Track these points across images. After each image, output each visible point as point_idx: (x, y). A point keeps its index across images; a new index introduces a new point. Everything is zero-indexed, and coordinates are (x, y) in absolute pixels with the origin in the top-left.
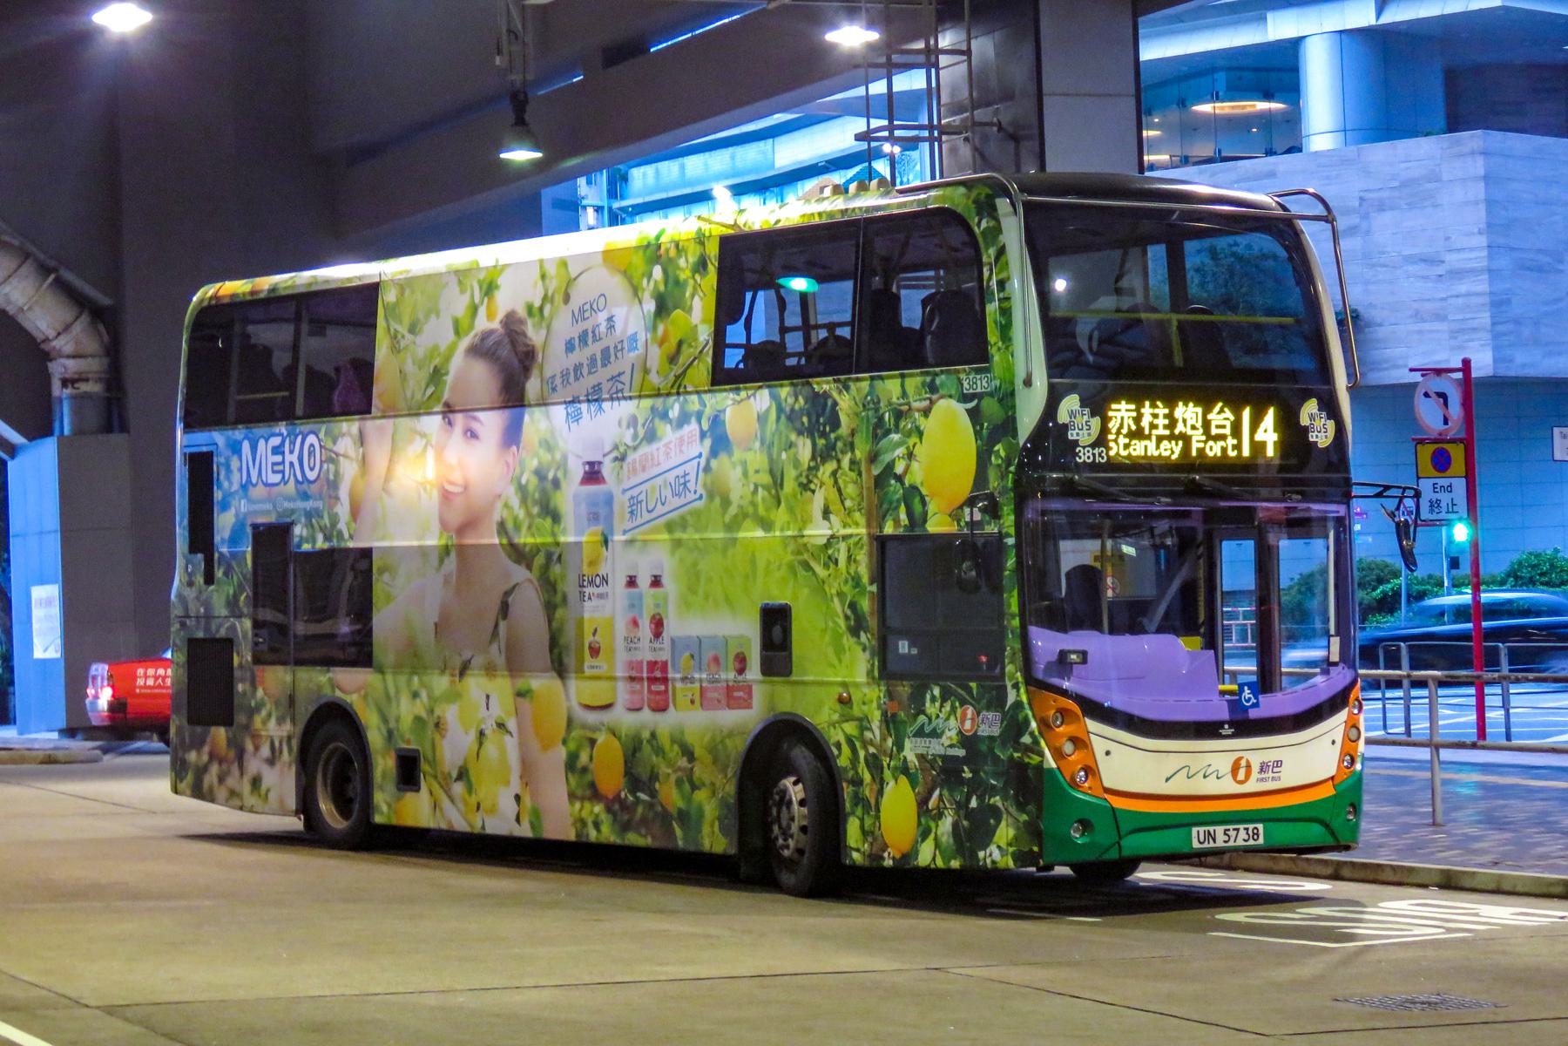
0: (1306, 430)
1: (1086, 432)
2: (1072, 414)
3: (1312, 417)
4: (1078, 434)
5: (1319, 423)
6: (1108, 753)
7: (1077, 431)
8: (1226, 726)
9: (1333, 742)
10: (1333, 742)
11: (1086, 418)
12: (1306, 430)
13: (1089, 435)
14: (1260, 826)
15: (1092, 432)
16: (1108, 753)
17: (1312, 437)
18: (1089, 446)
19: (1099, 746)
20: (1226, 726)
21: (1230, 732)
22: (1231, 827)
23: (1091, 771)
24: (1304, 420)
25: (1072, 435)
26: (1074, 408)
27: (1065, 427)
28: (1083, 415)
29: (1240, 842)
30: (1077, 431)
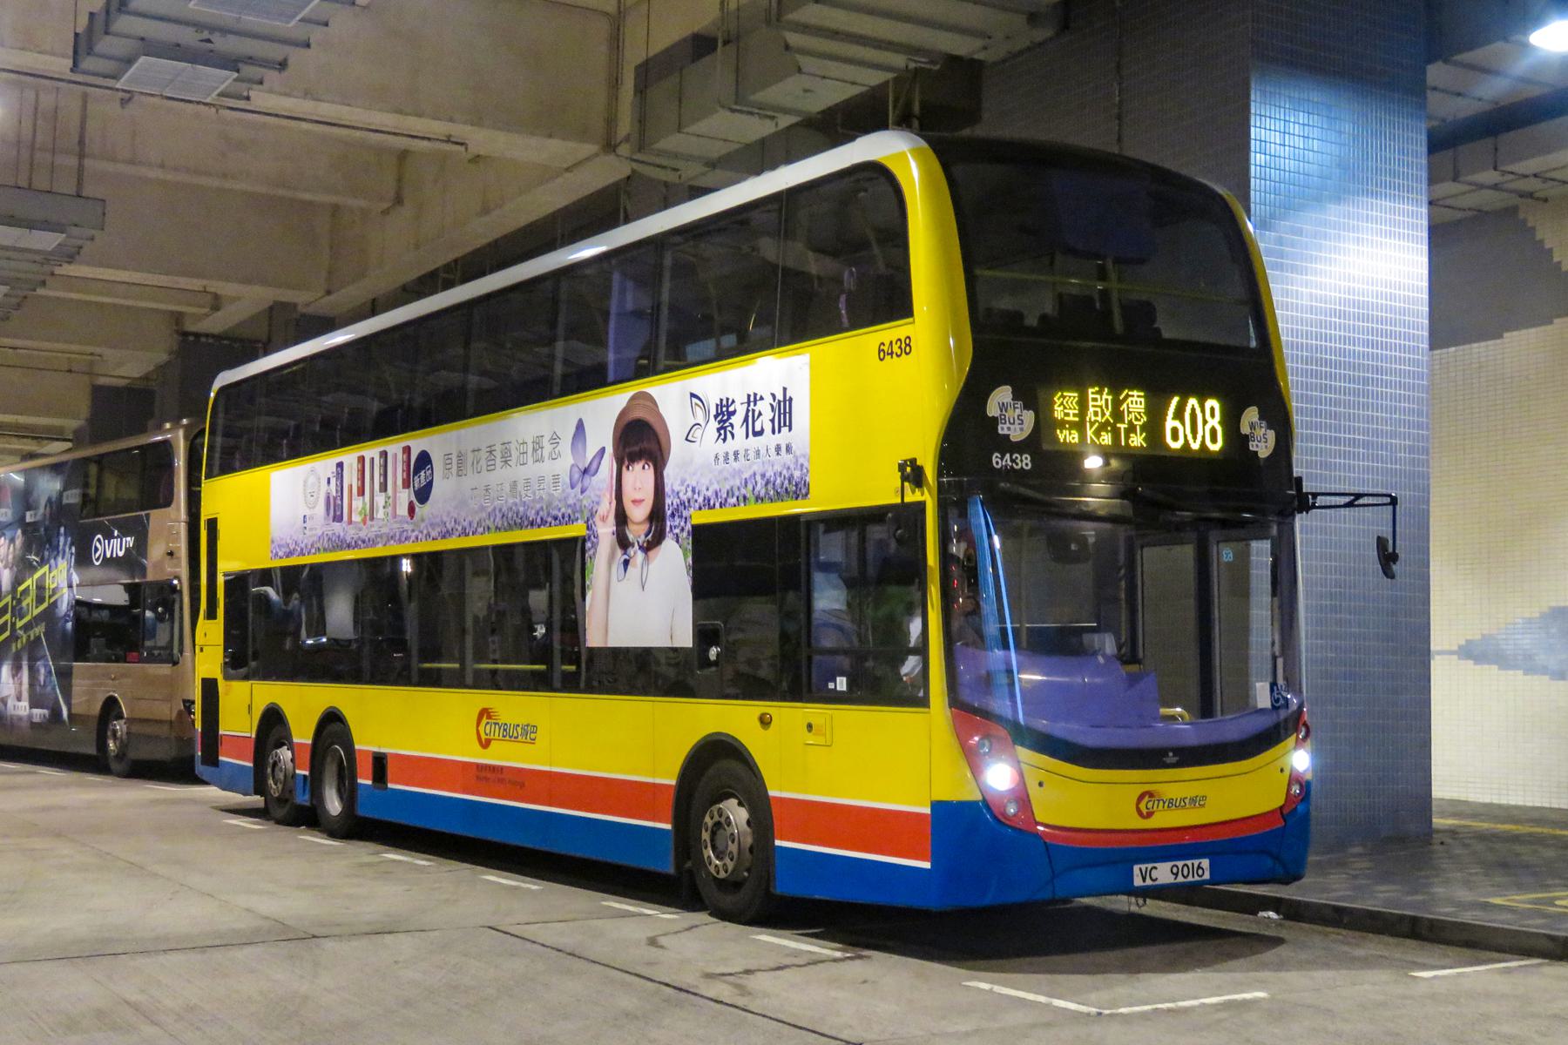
0: (1246, 439)
1: (1018, 427)
2: (1003, 407)
3: (1252, 426)
4: (1009, 429)
5: (1260, 432)
7: (1008, 425)
8: (1171, 754)
11: (1018, 411)
12: (1246, 439)
13: (1022, 429)
15: (1025, 426)
16: (1041, 784)
17: (1253, 446)
20: (1171, 754)
21: (1175, 760)
24: (1245, 429)
25: (1002, 429)
26: (1005, 401)
27: (995, 420)
28: (1015, 408)
30: (1008, 425)
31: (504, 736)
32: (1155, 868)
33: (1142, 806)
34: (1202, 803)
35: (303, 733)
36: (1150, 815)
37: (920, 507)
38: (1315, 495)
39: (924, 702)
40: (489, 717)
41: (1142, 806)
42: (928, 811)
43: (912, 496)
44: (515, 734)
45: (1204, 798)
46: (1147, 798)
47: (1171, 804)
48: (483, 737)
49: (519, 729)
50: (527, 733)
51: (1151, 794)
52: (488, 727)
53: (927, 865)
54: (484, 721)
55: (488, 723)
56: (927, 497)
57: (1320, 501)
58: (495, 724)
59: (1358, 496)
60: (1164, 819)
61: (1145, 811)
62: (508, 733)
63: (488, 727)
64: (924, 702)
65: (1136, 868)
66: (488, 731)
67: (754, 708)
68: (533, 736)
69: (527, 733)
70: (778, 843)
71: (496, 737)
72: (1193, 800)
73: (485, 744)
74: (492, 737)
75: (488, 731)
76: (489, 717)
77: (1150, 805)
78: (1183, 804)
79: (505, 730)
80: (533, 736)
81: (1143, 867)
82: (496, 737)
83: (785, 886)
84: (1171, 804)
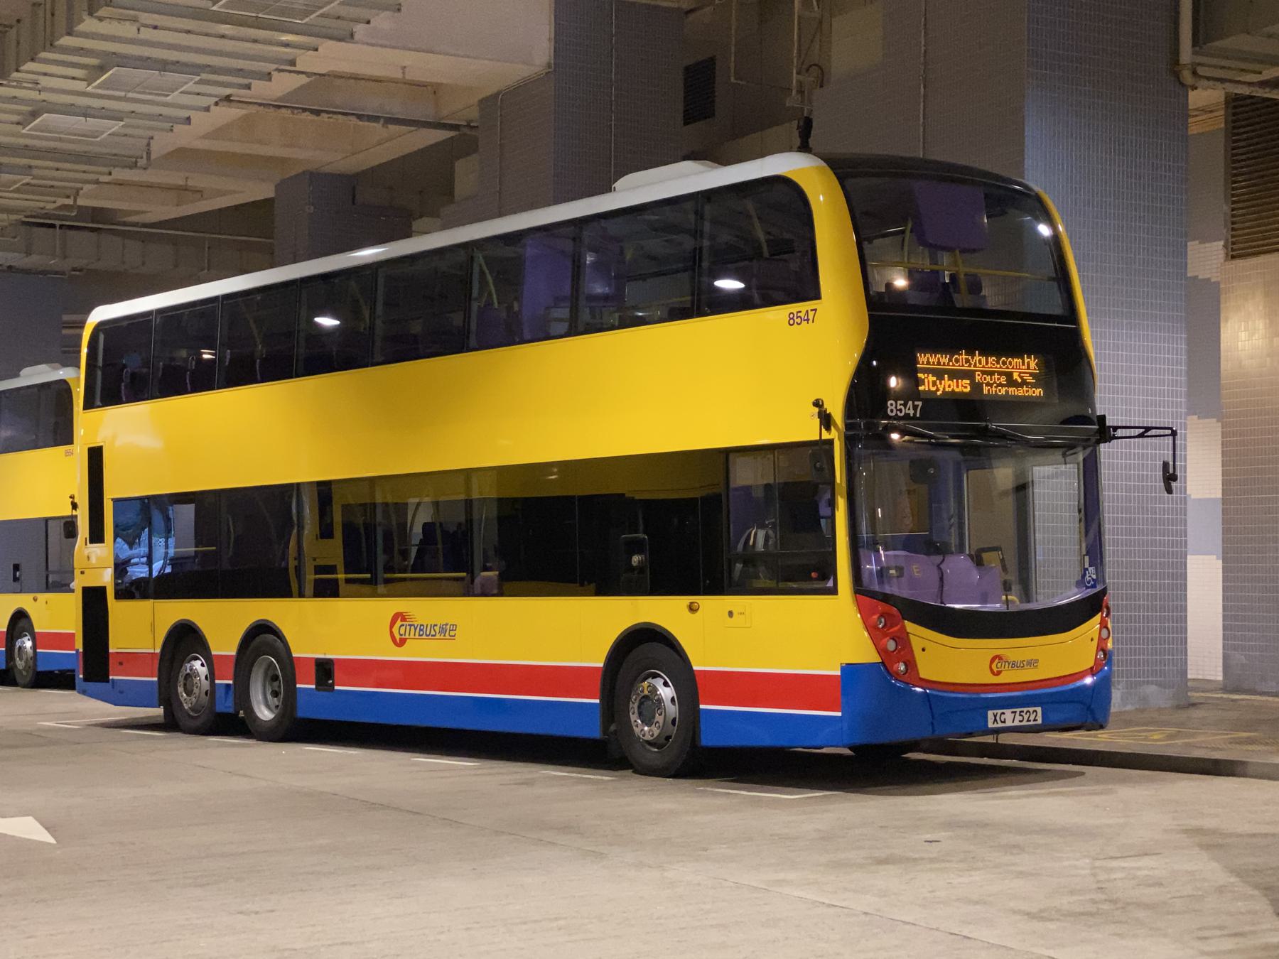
6: (923, 650)
9: (1092, 640)
10: (1092, 640)
14: (1039, 709)
16: (923, 650)
19: (916, 644)
22: (1018, 710)
23: (911, 664)
29: (1017, 723)
31: (420, 635)
32: (1003, 713)
33: (994, 666)
35: (224, 642)
36: (999, 673)
37: (830, 442)
38: (1115, 428)
39: (833, 591)
40: (404, 619)
41: (994, 666)
42: (839, 673)
43: (826, 436)
45: (1037, 661)
46: (997, 661)
47: (1014, 665)
48: (398, 637)
49: (437, 629)
50: (447, 631)
51: (999, 657)
52: (403, 628)
53: (839, 714)
56: (833, 435)
57: (1119, 433)
58: (410, 625)
59: (1148, 429)
60: (1008, 677)
61: (995, 670)
62: (424, 632)
63: (403, 628)
64: (833, 591)
65: (990, 713)
66: (402, 632)
67: (682, 602)
68: (452, 633)
69: (447, 631)
70: (702, 707)
71: (412, 636)
72: (1029, 663)
74: (407, 636)
75: (402, 632)
76: (404, 619)
77: (999, 664)
79: (420, 630)
80: (452, 633)
81: (995, 712)
82: (412, 636)
83: (709, 739)
84: (1014, 665)
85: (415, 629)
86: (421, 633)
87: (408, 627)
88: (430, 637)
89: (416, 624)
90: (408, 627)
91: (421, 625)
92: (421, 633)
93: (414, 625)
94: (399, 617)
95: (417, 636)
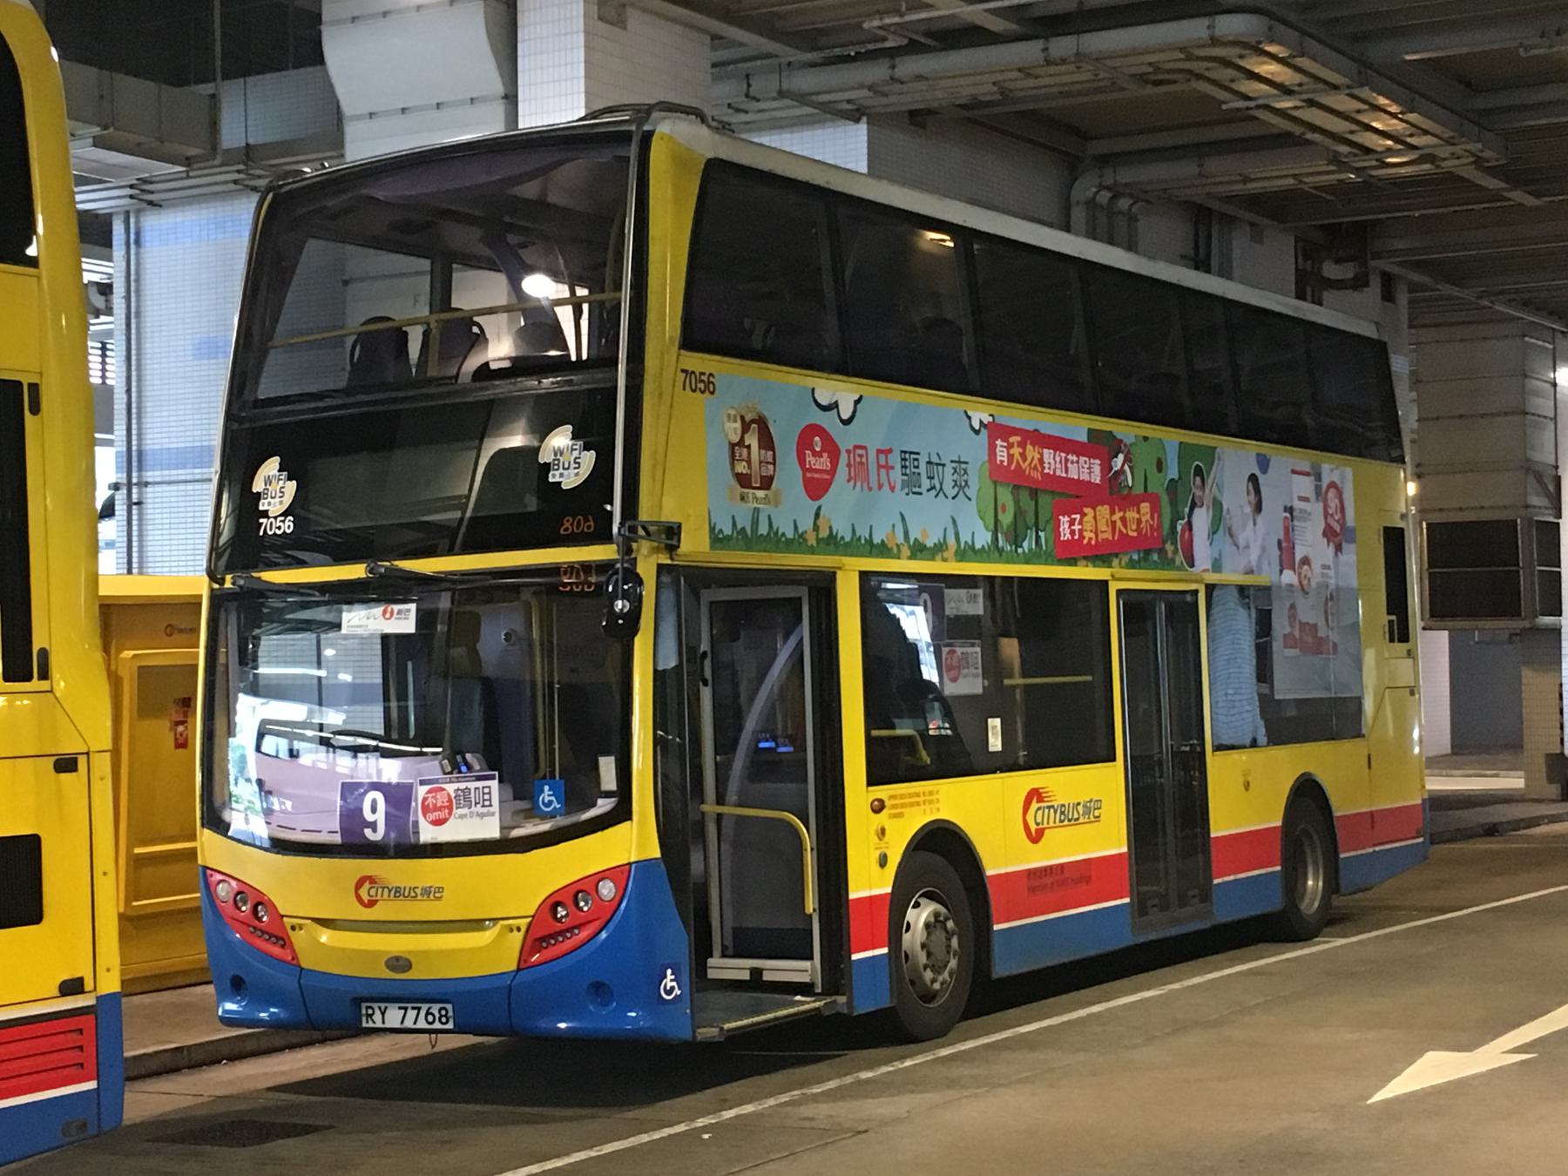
18: (281, 515)
31: (1061, 821)
34: (437, 895)
40: (1040, 800)
41: (363, 892)
44: (1076, 816)
46: (367, 885)
52: (1040, 812)
54: (1034, 806)
55: (1039, 809)
58: (1049, 807)
62: (1067, 816)
71: (1051, 824)
73: (1036, 837)
74: (1045, 825)
77: (373, 892)
78: (414, 895)
79: (1062, 813)
82: (1051, 824)
85: (1055, 812)
86: (1063, 817)
87: (1046, 811)
88: (1073, 822)
89: (1055, 804)
90: (1046, 811)
91: (1063, 805)
92: (1063, 817)
93: (1053, 807)
94: (1035, 795)
95: (1058, 823)
